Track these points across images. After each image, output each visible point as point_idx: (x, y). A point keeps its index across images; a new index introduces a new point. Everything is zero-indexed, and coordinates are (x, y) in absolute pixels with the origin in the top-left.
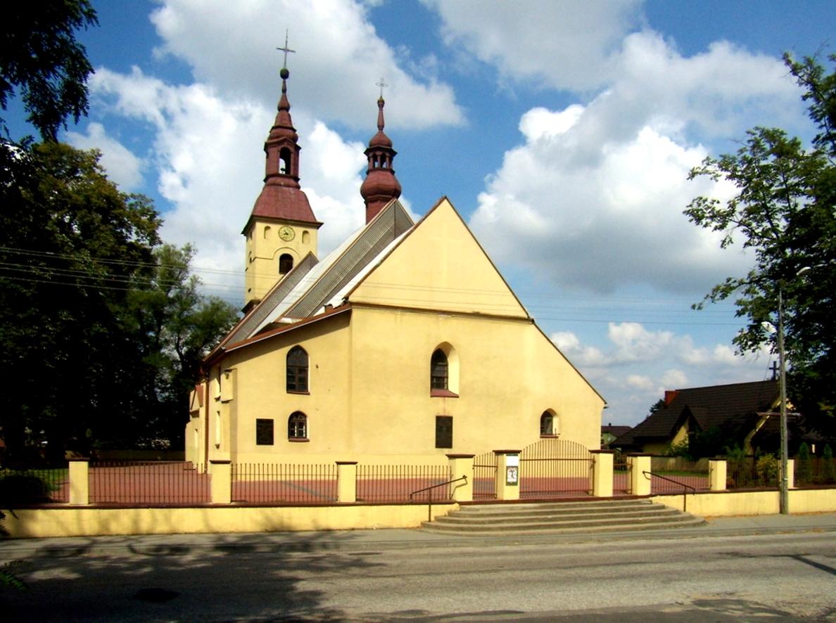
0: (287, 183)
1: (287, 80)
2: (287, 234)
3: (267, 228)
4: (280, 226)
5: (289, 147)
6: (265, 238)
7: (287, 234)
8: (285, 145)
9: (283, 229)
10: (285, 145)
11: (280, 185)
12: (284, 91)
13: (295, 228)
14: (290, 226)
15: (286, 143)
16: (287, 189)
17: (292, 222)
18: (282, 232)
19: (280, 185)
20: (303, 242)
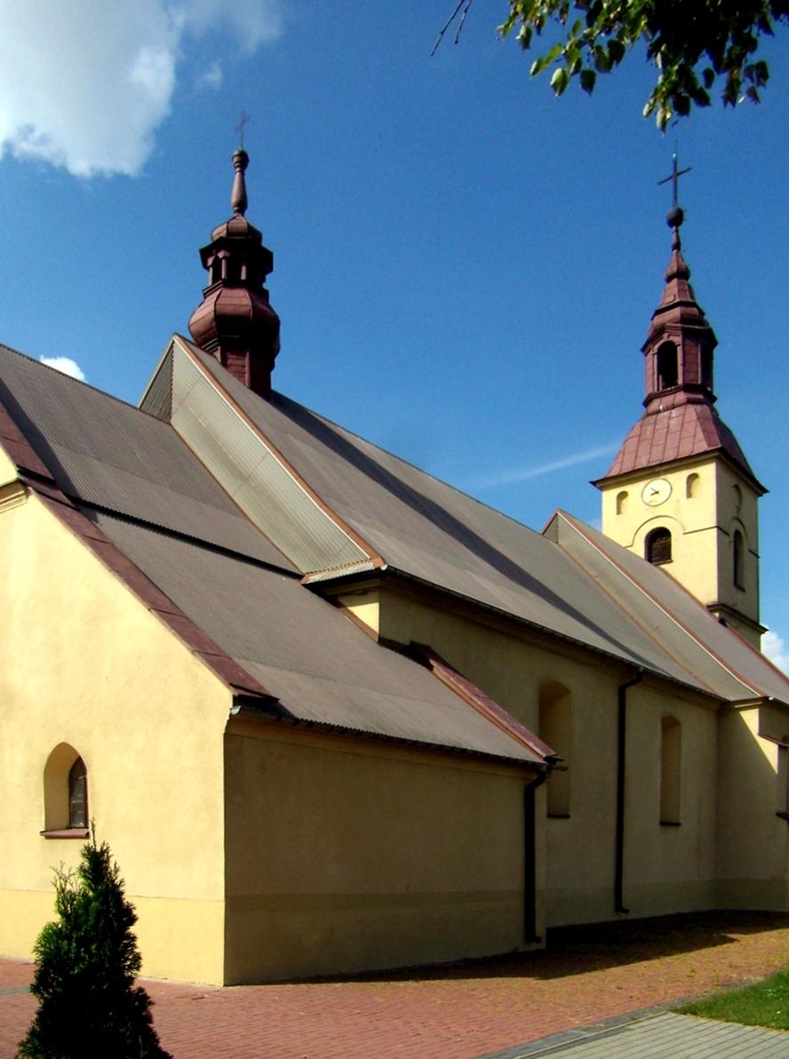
0: (670, 403)
1: (680, 228)
2: (657, 492)
3: (623, 496)
4: (641, 485)
5: (672, 338)
6: (619, 512)
7: (657, 492)
8: (665, 339)
9: (649, 485)
10: (665, 339)
11: (659, 412)
12: (677, 246)
13: (672, 477)
14: (663, 477)
15: (665, 335)
16: (665, 413)
17: (663, 468)
18: (648, 491)
19: (659, 412)
20: (689, 495)
